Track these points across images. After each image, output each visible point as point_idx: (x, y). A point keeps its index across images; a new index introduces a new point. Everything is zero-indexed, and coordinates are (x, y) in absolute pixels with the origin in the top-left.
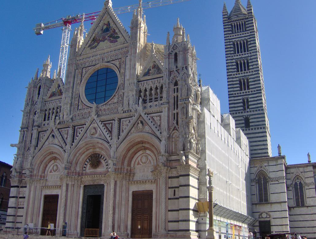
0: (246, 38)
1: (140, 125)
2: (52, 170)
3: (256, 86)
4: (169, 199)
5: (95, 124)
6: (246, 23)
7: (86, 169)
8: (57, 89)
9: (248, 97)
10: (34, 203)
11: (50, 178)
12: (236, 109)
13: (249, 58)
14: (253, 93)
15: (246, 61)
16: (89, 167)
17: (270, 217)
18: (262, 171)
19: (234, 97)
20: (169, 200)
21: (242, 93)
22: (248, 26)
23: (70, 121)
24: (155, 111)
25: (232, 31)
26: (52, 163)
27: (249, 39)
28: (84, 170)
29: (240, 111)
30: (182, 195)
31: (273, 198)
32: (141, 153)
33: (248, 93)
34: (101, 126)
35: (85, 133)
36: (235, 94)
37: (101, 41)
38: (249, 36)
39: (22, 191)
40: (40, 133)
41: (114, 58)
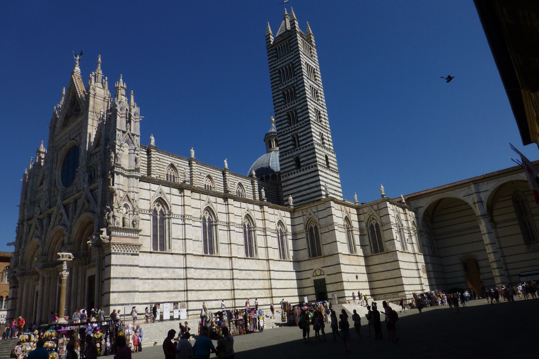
0: (291, 61)
1: (86, 204)
3: (305, 116)
6: (291, 42)
9: (297, 132)
10: (27, 302)
12: (286, 149)
13: (295, 85)
14: (302, 126)
15: (292, 89)
17: (324, 274)
18: (312, 219)
19: (283, 135)
21: (291, 129)
22: (292, 45)
25: (277, 56)
27: (294, 61)
29: (290, 151)
31: (326, 250)
33: (297, 128)
36: (284, 132)
38: (294, 57)
41: (76, 134)
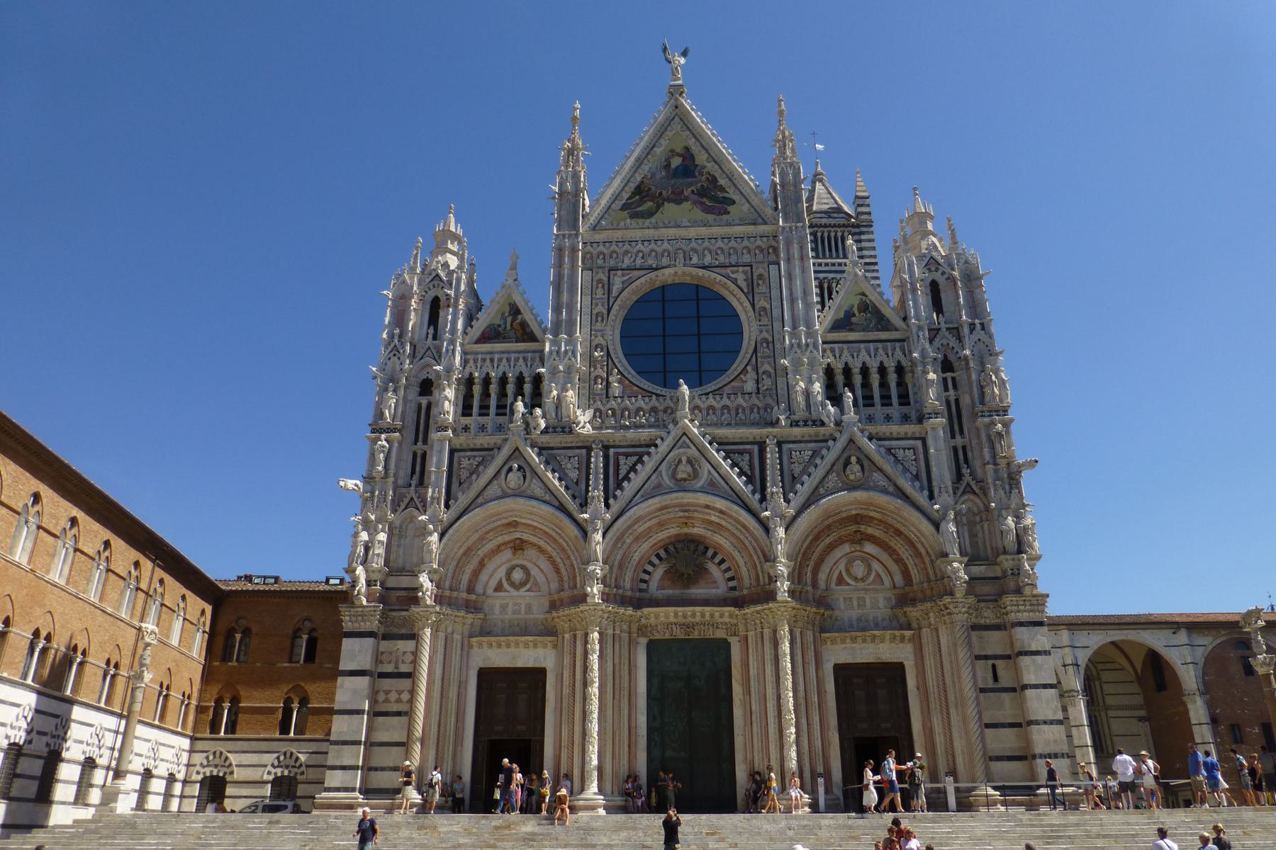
2: (506, 585)
4: (982, 690)
5: (689, 447)
7: (648, 586)
8: (509, 320)
11: (497, 610)
16: (662, 578)
20: (982, 694)
23: (588, 425)
24: (898, 433)
26: (504, 559)
28: (641, 590)
30: (1034, 682)
32: (849, 551)
34: (718, 457)
35: (654, 472)
37: (669, 200)
39: (391, 653)
40: (456, 455)
